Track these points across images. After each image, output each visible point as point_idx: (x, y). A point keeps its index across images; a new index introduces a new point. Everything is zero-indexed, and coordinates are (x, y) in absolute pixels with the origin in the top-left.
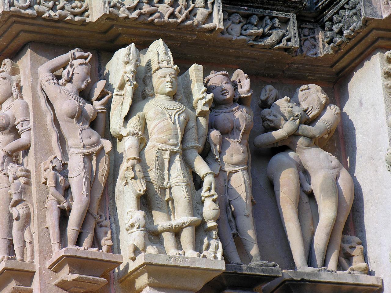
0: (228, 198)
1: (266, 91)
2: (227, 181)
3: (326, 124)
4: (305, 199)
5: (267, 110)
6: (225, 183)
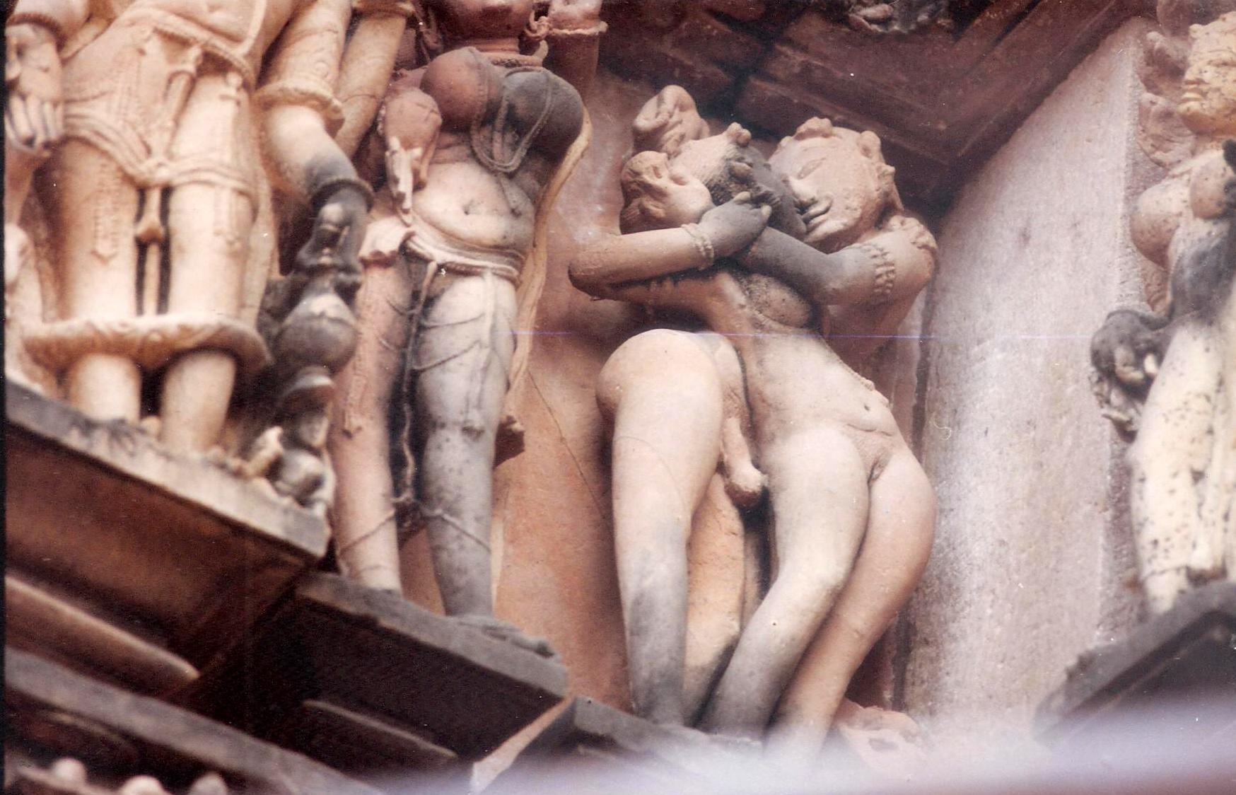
0: (412, 365)
1: (661, 101)
2: (422, 299)
3: (875, 256)
4: (727, 518)
5: (649, 158)
6: (412, 308)
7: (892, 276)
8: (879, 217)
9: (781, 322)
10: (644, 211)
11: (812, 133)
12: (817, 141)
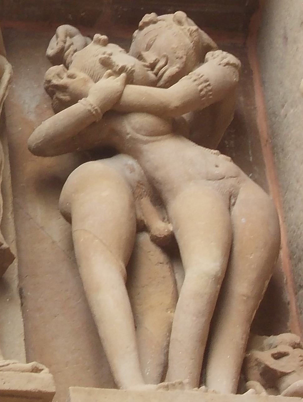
7: (209, 88)
8: (200, 55)
9: (151, 135)
10: (60, 100)
11: (147, 24)
12: (151, 26)
